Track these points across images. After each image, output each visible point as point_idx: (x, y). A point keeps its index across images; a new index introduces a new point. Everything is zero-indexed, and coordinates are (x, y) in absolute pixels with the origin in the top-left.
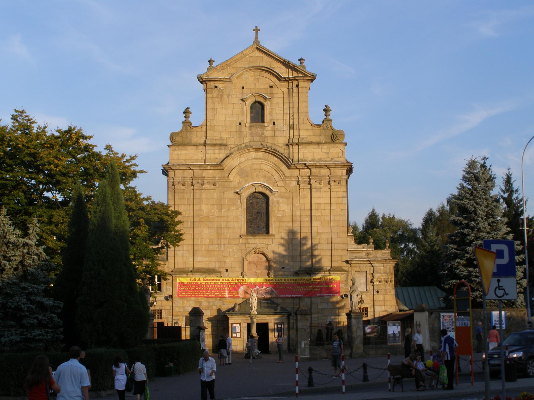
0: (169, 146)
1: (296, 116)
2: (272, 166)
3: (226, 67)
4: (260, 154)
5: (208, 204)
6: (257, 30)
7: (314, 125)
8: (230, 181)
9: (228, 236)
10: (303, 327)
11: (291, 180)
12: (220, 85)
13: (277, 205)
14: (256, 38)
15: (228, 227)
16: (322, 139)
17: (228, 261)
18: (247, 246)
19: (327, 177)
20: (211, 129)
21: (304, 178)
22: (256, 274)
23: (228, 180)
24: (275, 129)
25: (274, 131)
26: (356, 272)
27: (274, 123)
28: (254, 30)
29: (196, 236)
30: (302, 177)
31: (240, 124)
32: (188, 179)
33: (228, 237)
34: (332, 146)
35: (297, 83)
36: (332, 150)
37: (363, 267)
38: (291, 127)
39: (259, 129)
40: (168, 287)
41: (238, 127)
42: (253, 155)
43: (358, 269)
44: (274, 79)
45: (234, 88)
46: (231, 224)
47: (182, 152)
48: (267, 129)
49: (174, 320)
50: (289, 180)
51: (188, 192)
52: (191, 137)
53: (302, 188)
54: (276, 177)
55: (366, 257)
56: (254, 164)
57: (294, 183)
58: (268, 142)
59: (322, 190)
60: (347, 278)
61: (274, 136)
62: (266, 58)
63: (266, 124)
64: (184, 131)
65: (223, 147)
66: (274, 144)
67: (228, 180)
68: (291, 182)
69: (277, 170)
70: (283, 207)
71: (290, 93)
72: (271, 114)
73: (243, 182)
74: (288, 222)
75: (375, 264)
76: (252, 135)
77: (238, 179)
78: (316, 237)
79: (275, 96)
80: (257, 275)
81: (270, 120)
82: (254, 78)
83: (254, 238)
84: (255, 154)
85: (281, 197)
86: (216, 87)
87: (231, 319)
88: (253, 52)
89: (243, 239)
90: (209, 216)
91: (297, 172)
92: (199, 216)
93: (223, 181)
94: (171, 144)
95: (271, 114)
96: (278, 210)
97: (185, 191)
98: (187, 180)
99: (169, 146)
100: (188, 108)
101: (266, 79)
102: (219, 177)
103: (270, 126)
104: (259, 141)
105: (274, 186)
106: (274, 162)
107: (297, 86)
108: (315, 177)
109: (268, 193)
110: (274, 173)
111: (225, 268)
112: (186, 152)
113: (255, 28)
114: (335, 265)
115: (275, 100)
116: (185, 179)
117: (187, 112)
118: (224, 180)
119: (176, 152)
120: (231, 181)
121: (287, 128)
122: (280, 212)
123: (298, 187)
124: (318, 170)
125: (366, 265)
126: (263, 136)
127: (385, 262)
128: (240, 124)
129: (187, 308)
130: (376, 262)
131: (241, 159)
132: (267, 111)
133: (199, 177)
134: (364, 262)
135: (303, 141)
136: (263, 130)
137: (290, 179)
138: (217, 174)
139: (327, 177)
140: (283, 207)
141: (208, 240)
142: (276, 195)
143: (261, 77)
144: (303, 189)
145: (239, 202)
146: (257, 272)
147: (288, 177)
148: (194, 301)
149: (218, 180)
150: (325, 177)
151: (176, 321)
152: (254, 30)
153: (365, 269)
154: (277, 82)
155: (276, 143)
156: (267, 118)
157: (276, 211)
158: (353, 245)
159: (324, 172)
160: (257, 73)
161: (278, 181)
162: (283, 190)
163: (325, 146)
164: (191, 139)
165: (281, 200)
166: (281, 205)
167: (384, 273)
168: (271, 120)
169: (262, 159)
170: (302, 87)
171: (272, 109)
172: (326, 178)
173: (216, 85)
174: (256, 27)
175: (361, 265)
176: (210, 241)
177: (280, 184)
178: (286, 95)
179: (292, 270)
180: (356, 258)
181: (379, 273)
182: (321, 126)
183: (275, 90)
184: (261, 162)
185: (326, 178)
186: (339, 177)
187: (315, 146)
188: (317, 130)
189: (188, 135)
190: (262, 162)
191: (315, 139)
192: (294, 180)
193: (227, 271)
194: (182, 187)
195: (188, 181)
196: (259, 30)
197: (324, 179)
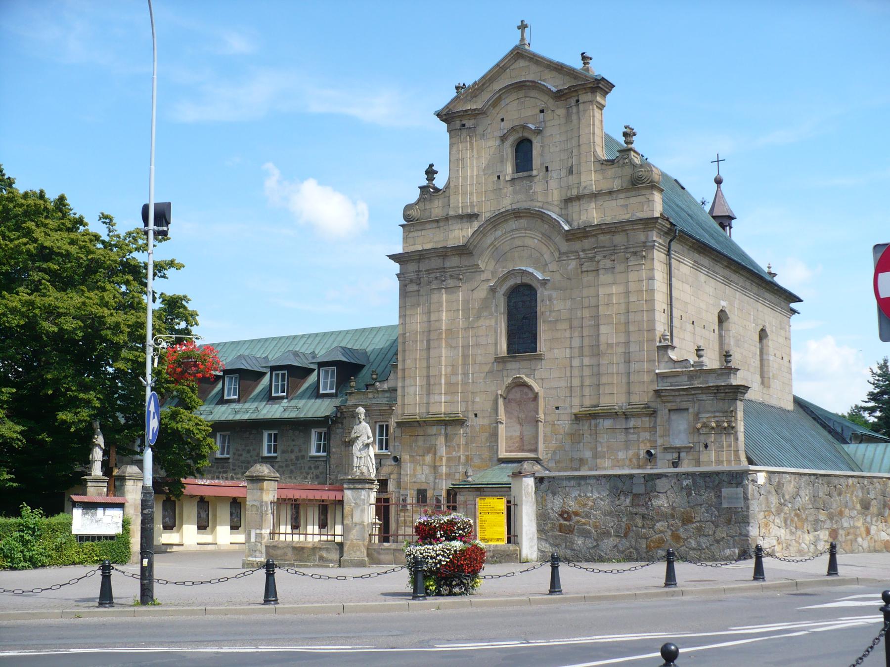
0: (402, 226)
1: (575, 152)
2: (540, 239)
3: (478, 93)
4: (523, 222)
5: (450, 311)
6: (523, 27)
7: (604, 163)
8: (480, 270)
9: (479, 359)
10: (255, 503)
11: (569, 258)
12: (469, 123)
13: (548, 303)
14: (523, 39)
15: (477, 345)
16: (616, 185)
17: (477, 399)
18: (505, 373)
19: (622, 247)
20: (455, 192)
21: (588, 252)
22: (519, 420)
23: (478, 270)
24: (548, 178)
25: (547, 182)
26: (672, 413)
27: (547, 168)
28: (519, 28)
29: (432, 361)
30: (583, 251)
31: (499, 177)
32: (423, 274)
33: (478, 362)
34: (633, 193)
35: (576, 98)
36: (632, 200)
37: (680, 402)
38: (571, 172)
39: (525, 182)
40: (396, 444)
41: (495, 182)
42: (513, 224)
43: (673, 406)
44: (545, 98)
45: (490, 122)
46: (483, 341)
47: (420, 233)
48: (536, 179)
49: (402, 495)
50: (566, 258)
51: (424, 294)
52: (431, 209)
53: (586, 269)
54: (547, 257)
55: (688, 383)
56: (514, 238)
57: (573, 264)
58: (538, 201)
59: (617, 270)
60: (655, 422)
61: (547, 190)
62: (534, 67)
63: (535, 173)
64: (422, 200)
65: (474, 218)
66: (547, 203)
67: (478, 270)
68: (570, 261)
69: (547, 244)
70: (558, 305)
71: (568, 116)
72: (542, 155)
73: (500, 270)
74: (565, 330)
75: (701, 396)
76: (515, 192)
77: (491, 265)
78: (604, 352)
79: (548, 124)
80: (521, 421)
81: (541, 165)
82: (517, 101)
83: (516, 361)
84: (516, 222)
85: (555, 289)
86: (464, 125)
87: (460, 495)
88: (516, 61)
89: (499, 362)
90: (452, 329)
91: (577, 245)
92: (436, 330)
93: (472, 272)
94: (405, 223)
95: (542, 155)
96: (550, 311)
97: (421, 293)
98: (422, 276)
99: (402, 226)
100: (431, 166)
101: (534, 100)
102: (465, 266)
103: (541, 175)
104: (525, 201)
105: (543, 272)
106: (544, 231)
107: (578, 101)
108: (602, 249)
109: (535, 284)
110: (544, 250)
111: (474, 411)
112: (424, 233)
113: (520, 24)
114: (635, 399)
115: (547, 132)
116: (420, 273)
117: (431, 173)
118: (473, 270)
119: (411, 235)
120: (483, 271)
121: (564, 173)
122: (554, 314)
123: (579, 270)
124: (608, 237)
125: (685, 398)
126: (531, 191)
127: (715, 391)
128: (499, 177)
129: (419, 476)
130: (700, 392)
131: (497, 233)
132: (535, 152)
133: (437, 269)
134: (682, 393)
135: (587, 192)
136: (531, 182)
137: (567, 257)
138: (466, 261)
139: (622, 247)
140: (558, 305)
141: (451, 368)
142: (547, 286)
143: (528, 99)
144: (587, 271)
145: (494, 304)
146: (520, 416)
147: (564, 253)
148: (429, 466)
149: (465, 271)
150: (619, 248)
151: (404, 497)
152: (519, 28)
153: (684, 405)
154: (551, 102)
155: (549, 200)
156: (536, 162)
157: (548, 313)
158: (667, 362)
159: (619, 239)
160: (521, 94)
161: (550, 263)
162: (557, 277)
163: (622, 196)
164: (431, 212)
165: (554, 294)
166: (555, 302)
167: (718, 412)
168: (542, 164)
169: (525, 230)
170: (584, 103)
171: (543, 147)
172: (621, 249)
173: (463, 122)
174: (522, 22)
175: (679, 399)
176: (453, 368)
177: (553, 267)
178: (563, 121)
179: (569, 411)
180: (671, 386)
181: (709, 412)
182: (616, 161)
183: (548, 113)
184: (524, 235)
185: (621, 249)
186: (641, 245)
187: (606, 198)
188: (611, 172)
189: (427, 207)
190: (527, 235)
191: (605, 186)
192: (574, 257)
193: (476, 415)
194: (415, 288)
195: (423, 277)
196: (526, 26)
197: (618, 251)
